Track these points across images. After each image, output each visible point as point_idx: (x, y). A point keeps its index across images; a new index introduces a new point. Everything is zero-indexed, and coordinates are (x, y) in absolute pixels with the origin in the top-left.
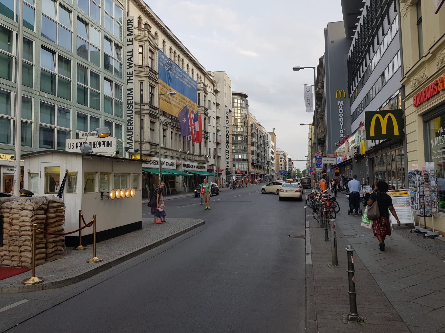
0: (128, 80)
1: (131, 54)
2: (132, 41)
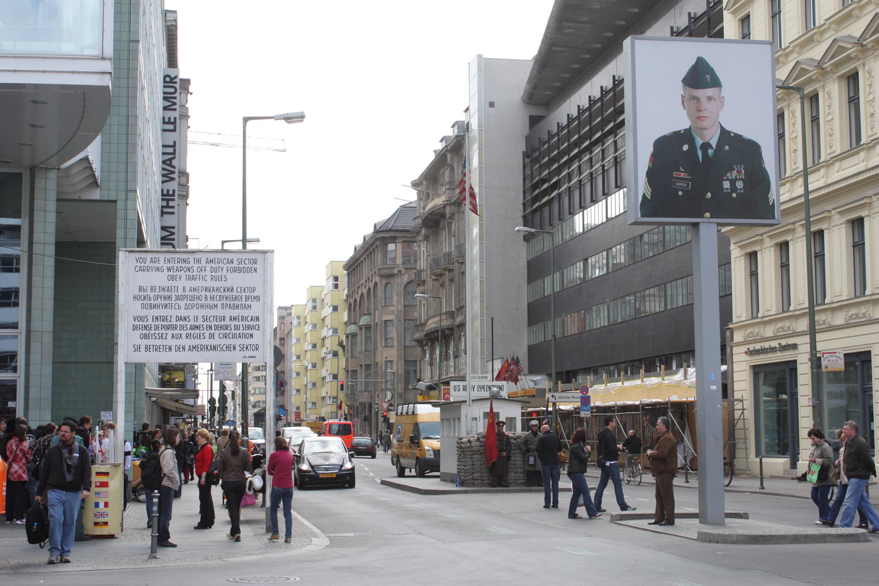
0: (163, 207)
1: (171, 150)
2: (174, 123)
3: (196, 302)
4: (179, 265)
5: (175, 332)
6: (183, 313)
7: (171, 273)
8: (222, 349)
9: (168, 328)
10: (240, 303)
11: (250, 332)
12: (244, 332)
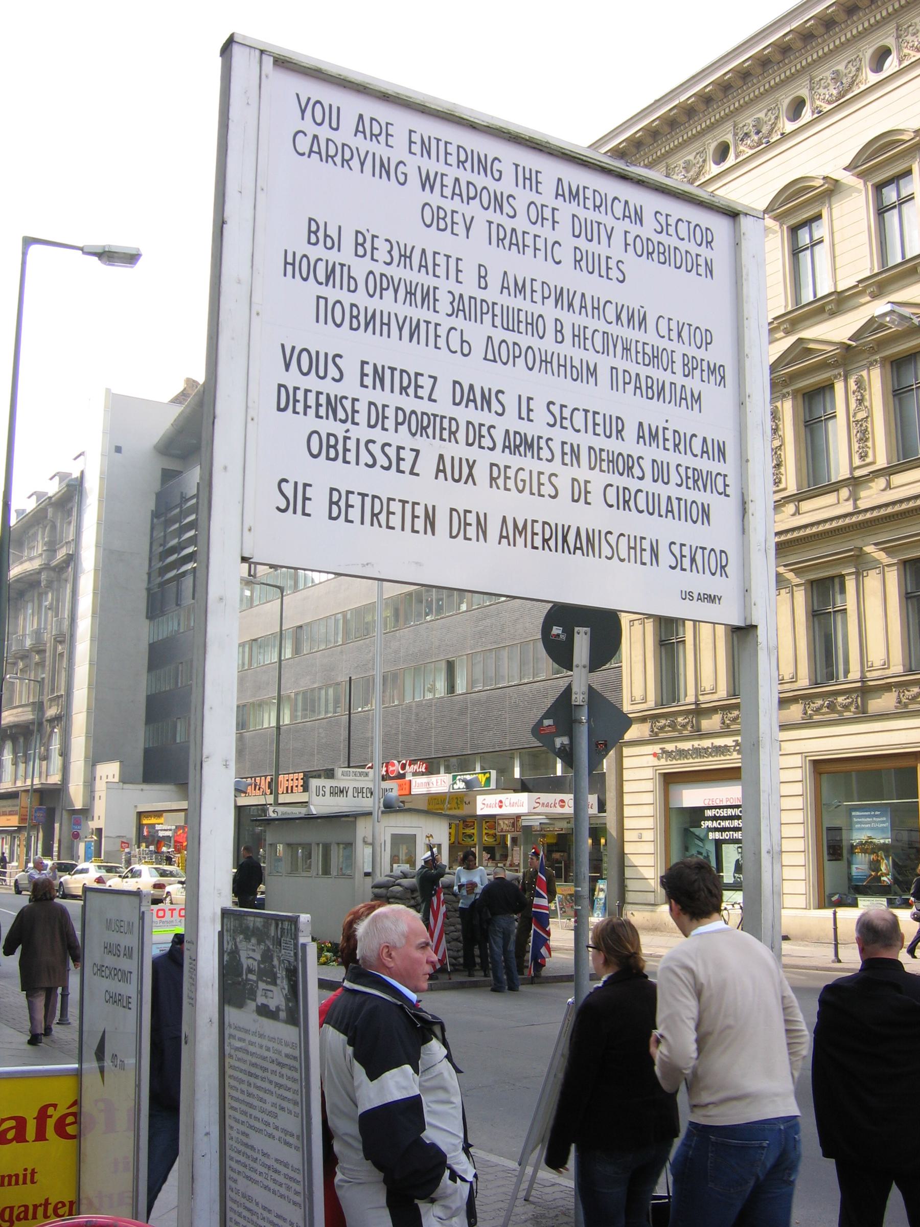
3: (525, 341)
4: (465, 176)
5: (452, 450)
6: (480, 374)
7: (435, 199)
8: (615, 550)
9: (423, 425)
10: (667, 377)
11: (701, 497)
12: (683, 492)
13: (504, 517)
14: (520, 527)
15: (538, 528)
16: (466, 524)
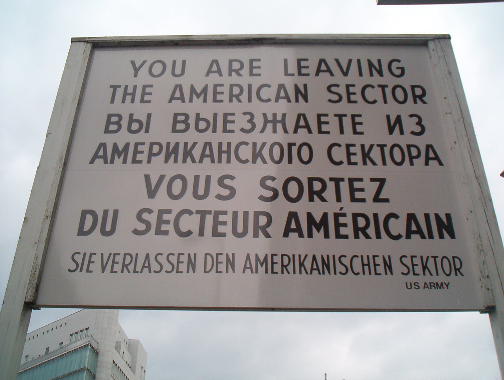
13: (248, 255)
14: (262, 259)
15: (277, 259)
16: (218, 263)
